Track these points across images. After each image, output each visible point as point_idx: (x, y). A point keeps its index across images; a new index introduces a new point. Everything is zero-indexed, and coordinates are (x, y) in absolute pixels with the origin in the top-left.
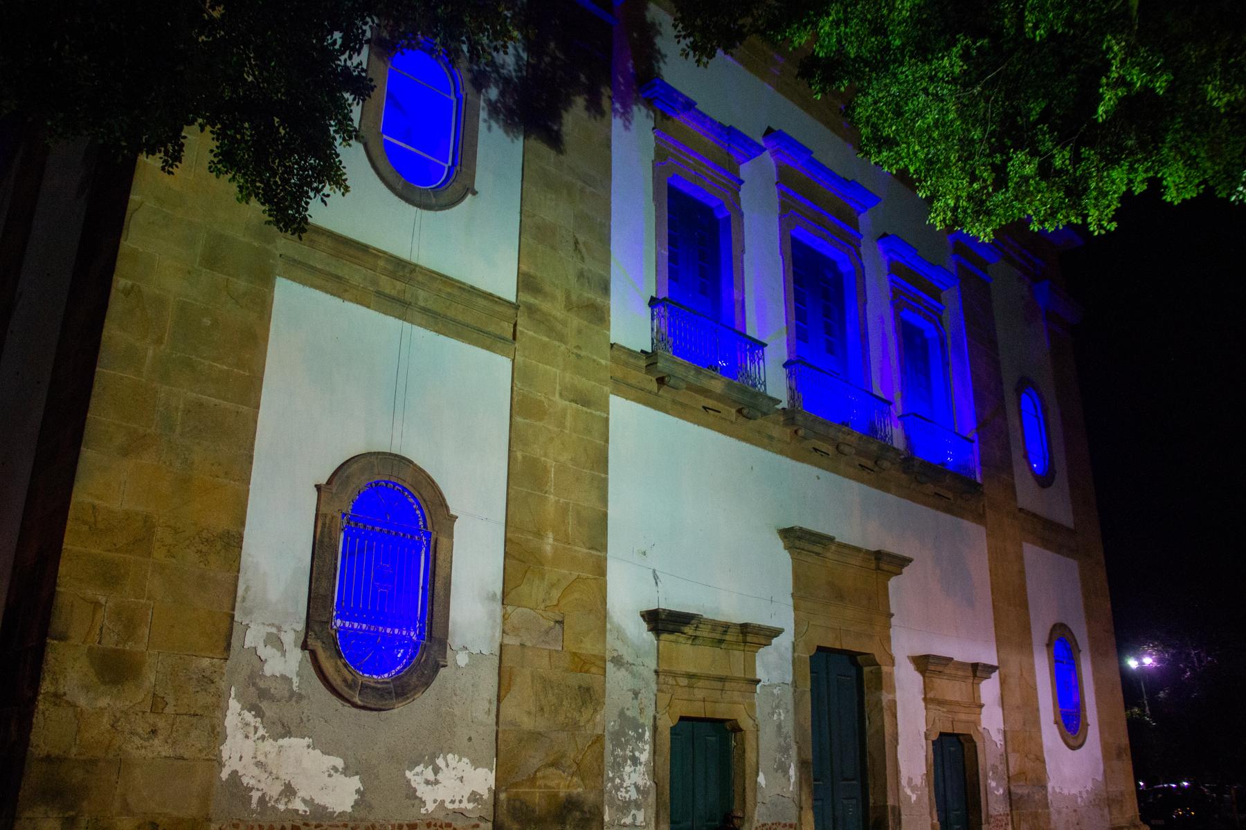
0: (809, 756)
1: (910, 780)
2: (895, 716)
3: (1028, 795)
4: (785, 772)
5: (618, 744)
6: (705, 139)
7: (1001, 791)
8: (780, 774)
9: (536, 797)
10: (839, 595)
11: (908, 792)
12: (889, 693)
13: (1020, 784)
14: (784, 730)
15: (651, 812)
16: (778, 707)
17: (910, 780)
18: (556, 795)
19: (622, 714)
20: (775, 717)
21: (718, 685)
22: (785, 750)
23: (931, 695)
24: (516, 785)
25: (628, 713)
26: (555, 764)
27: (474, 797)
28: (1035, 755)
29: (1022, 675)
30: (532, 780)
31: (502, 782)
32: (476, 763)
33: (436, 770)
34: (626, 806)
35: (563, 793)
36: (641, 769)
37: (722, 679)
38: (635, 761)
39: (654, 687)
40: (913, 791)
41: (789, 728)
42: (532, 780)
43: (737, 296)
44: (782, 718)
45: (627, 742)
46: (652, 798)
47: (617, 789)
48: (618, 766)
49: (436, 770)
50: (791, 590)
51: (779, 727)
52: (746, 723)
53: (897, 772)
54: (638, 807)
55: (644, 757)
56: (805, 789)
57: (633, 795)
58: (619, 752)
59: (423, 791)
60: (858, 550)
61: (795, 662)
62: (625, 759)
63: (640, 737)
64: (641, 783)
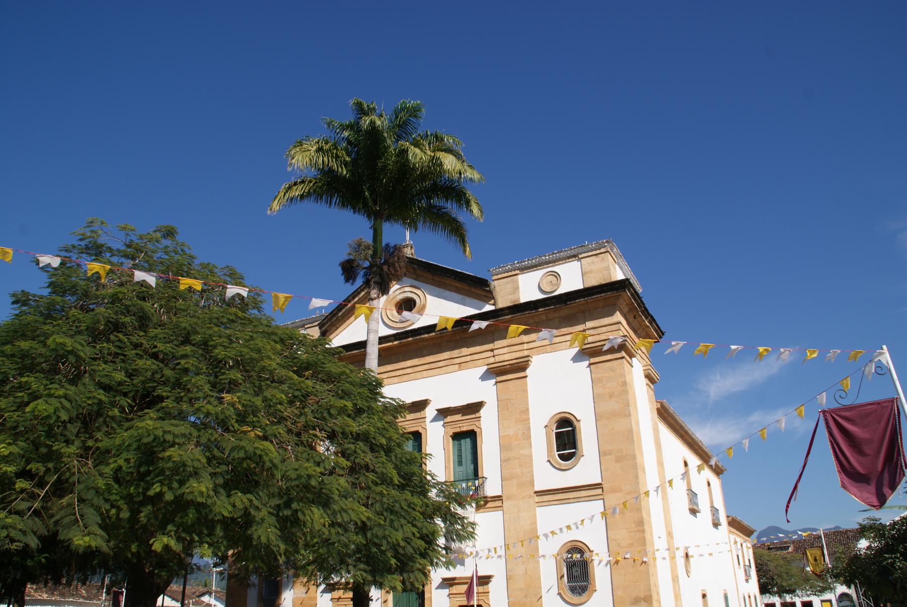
29: (526, 573)
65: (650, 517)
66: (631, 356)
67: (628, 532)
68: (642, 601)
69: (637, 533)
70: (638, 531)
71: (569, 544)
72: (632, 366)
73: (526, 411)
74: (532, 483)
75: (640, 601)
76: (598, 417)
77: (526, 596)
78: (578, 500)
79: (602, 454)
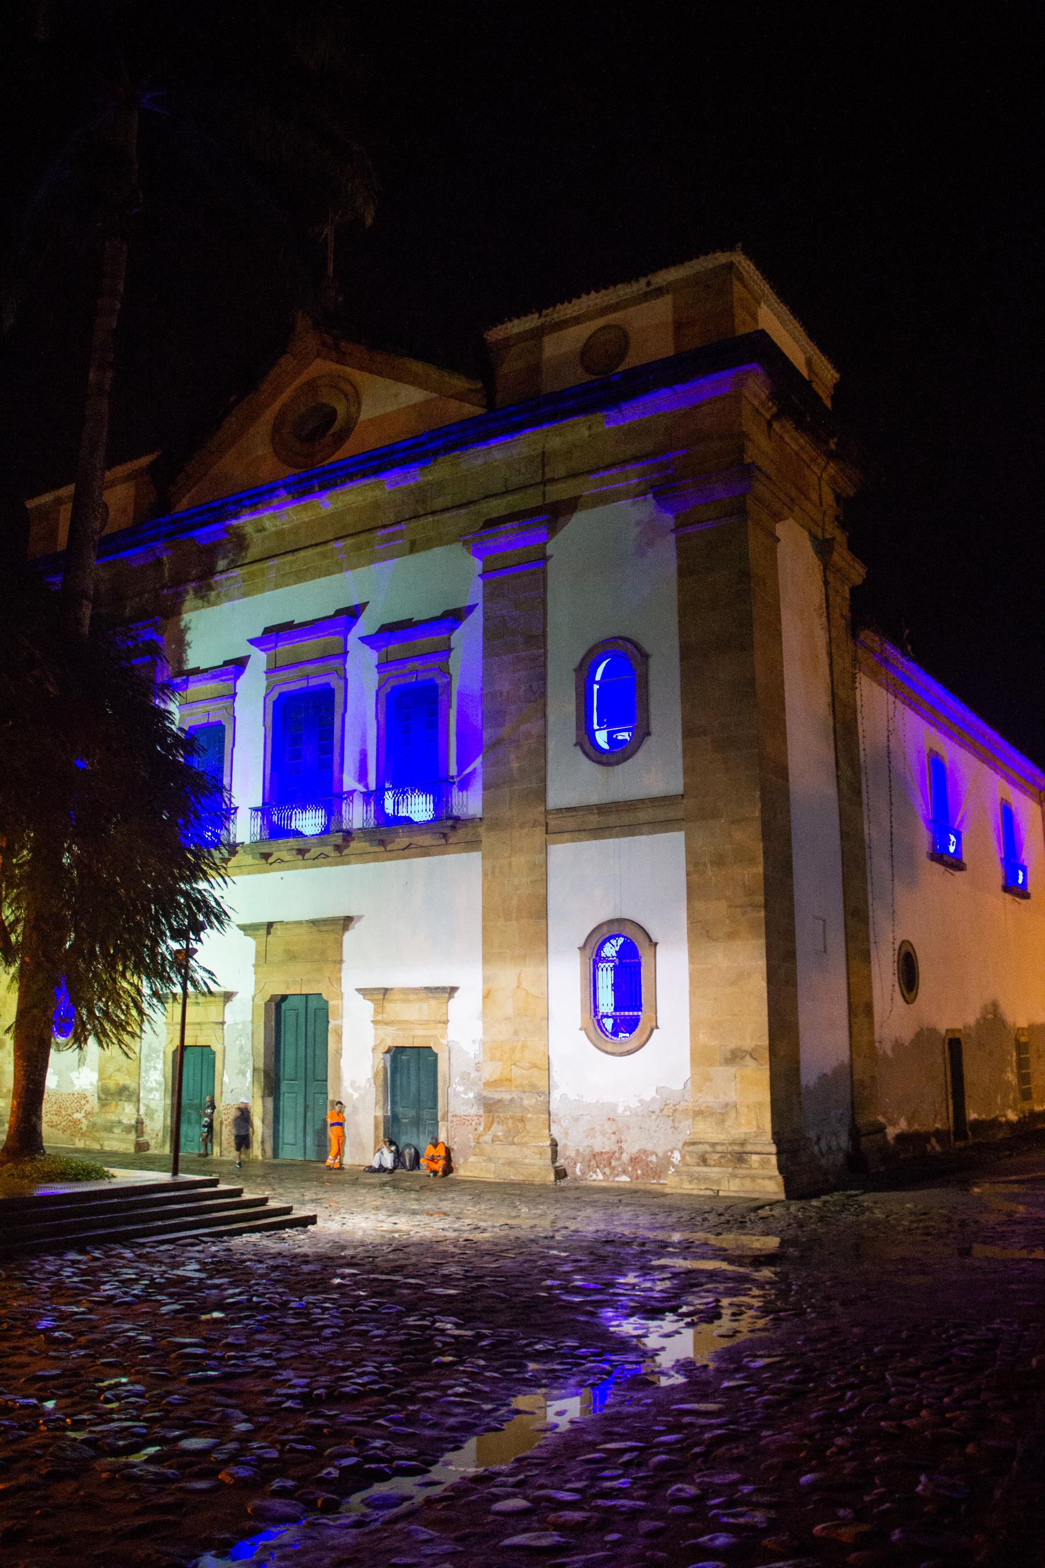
0: (261, 1064)
1: (353, 1083)
2: (339, 1036)
3: (512, 1100)
4: (244, 1075)
5: (147, 1061)
6: (209, 686)
7: (471, 1095)
8: (241, 1077)
9: (112, 1085)
10: (292, 956)
11: (351, 1091)
12: (335, 1019)
13: (499, 1089)
14: (246, 1050)
15: (163, 1093)
16: (240, 1036)
17: (353, 1083)
18: (118, 1084)
19: (150, 1046)
20: (238, 1042)
21: (199, 1027)
22: (244, 1062)
23: (379, 1018)
24: (104, 1079)
25: (153, 1046)
26: (119, 1070)
27: (91, 1084)
28: (530, 1063)
29: (518, 987)
30: (110, 1077)
31: (100, 1079)
32: (92, 1070)
33: (79, 1073)
34: (151, 1090)
35: (121, 1083)
36: (158, 1072)
37: (199, 1024)
38: (155, 1068)
39: (166, 1031)
40: (355, 1090)
41: (248, 1048)
42: (110, 1077)
43: (226, 781)
44: (243, 1042)
45: (152, 1059)
46: (163, 1087)
47: (147, 1082)
48: (147, 1071)
49: (79, 1073)
50: (253, 962)
51: (241, 1048)
52: (216, 1047)
53: (338, 1078)
54: (157, 1090)
55: (160, 1066)
56: (256, 1084)
57: (154, 1085)
58: (148, 1064)
59: (75, 1081)
60: (300, 923)
61: (254, 1007)
62: (151, 1067)
63: (158, 1057)
64: (158, 1079)
65: (792, 877)
66: (778, 517)
67: (730, 906)
68: (748, 1058)
69: (749, 909)
70: (751, 905)
71: (605, 929)
72: (778, 540)
73: (538, 639)
74: (541, 794)
75: (742, 1058)
76: (686, 652)
77: (516, 1033)
78: (631, 830)
79: (689, 732)
